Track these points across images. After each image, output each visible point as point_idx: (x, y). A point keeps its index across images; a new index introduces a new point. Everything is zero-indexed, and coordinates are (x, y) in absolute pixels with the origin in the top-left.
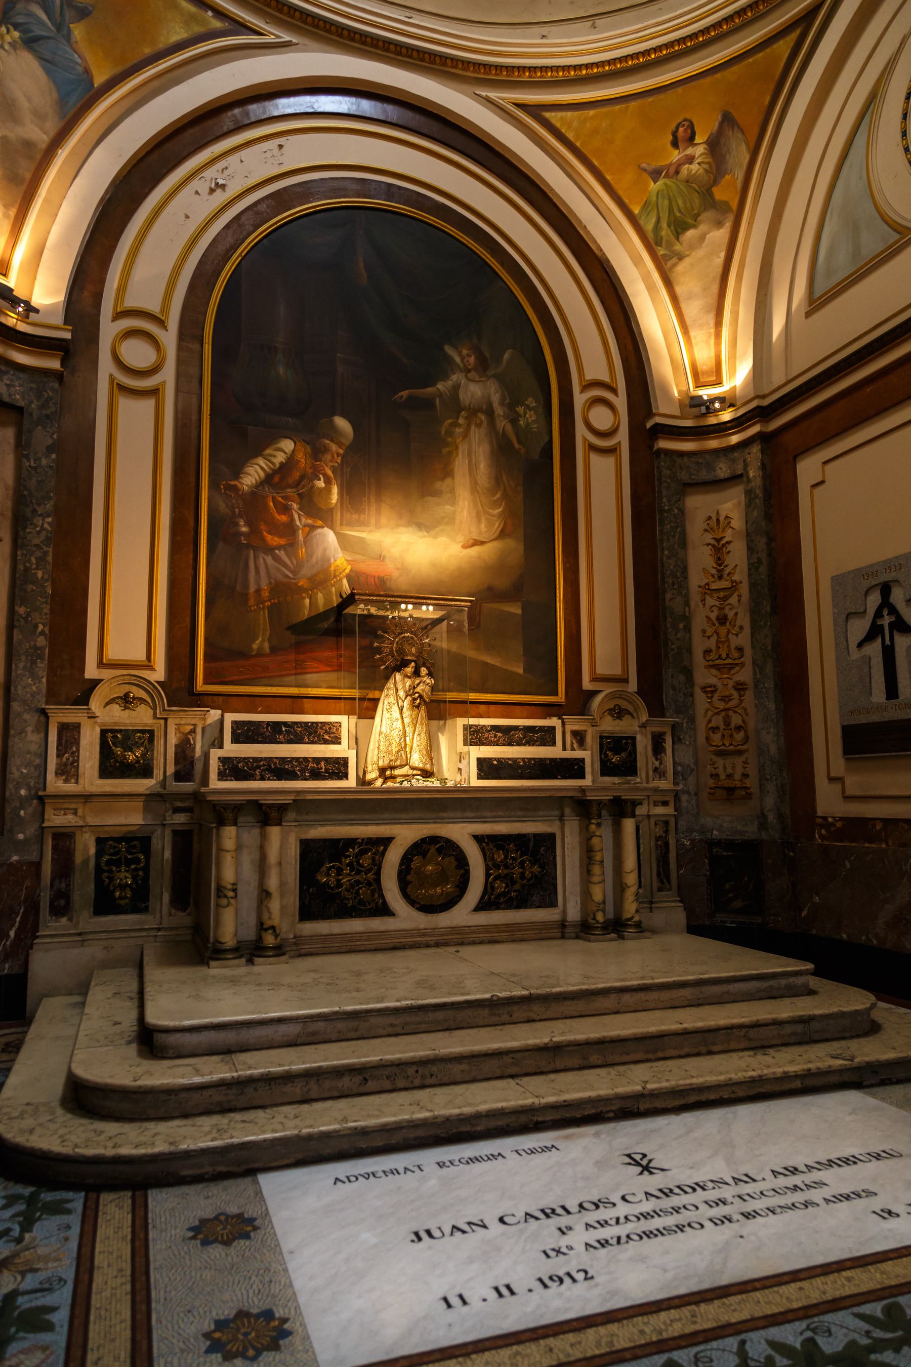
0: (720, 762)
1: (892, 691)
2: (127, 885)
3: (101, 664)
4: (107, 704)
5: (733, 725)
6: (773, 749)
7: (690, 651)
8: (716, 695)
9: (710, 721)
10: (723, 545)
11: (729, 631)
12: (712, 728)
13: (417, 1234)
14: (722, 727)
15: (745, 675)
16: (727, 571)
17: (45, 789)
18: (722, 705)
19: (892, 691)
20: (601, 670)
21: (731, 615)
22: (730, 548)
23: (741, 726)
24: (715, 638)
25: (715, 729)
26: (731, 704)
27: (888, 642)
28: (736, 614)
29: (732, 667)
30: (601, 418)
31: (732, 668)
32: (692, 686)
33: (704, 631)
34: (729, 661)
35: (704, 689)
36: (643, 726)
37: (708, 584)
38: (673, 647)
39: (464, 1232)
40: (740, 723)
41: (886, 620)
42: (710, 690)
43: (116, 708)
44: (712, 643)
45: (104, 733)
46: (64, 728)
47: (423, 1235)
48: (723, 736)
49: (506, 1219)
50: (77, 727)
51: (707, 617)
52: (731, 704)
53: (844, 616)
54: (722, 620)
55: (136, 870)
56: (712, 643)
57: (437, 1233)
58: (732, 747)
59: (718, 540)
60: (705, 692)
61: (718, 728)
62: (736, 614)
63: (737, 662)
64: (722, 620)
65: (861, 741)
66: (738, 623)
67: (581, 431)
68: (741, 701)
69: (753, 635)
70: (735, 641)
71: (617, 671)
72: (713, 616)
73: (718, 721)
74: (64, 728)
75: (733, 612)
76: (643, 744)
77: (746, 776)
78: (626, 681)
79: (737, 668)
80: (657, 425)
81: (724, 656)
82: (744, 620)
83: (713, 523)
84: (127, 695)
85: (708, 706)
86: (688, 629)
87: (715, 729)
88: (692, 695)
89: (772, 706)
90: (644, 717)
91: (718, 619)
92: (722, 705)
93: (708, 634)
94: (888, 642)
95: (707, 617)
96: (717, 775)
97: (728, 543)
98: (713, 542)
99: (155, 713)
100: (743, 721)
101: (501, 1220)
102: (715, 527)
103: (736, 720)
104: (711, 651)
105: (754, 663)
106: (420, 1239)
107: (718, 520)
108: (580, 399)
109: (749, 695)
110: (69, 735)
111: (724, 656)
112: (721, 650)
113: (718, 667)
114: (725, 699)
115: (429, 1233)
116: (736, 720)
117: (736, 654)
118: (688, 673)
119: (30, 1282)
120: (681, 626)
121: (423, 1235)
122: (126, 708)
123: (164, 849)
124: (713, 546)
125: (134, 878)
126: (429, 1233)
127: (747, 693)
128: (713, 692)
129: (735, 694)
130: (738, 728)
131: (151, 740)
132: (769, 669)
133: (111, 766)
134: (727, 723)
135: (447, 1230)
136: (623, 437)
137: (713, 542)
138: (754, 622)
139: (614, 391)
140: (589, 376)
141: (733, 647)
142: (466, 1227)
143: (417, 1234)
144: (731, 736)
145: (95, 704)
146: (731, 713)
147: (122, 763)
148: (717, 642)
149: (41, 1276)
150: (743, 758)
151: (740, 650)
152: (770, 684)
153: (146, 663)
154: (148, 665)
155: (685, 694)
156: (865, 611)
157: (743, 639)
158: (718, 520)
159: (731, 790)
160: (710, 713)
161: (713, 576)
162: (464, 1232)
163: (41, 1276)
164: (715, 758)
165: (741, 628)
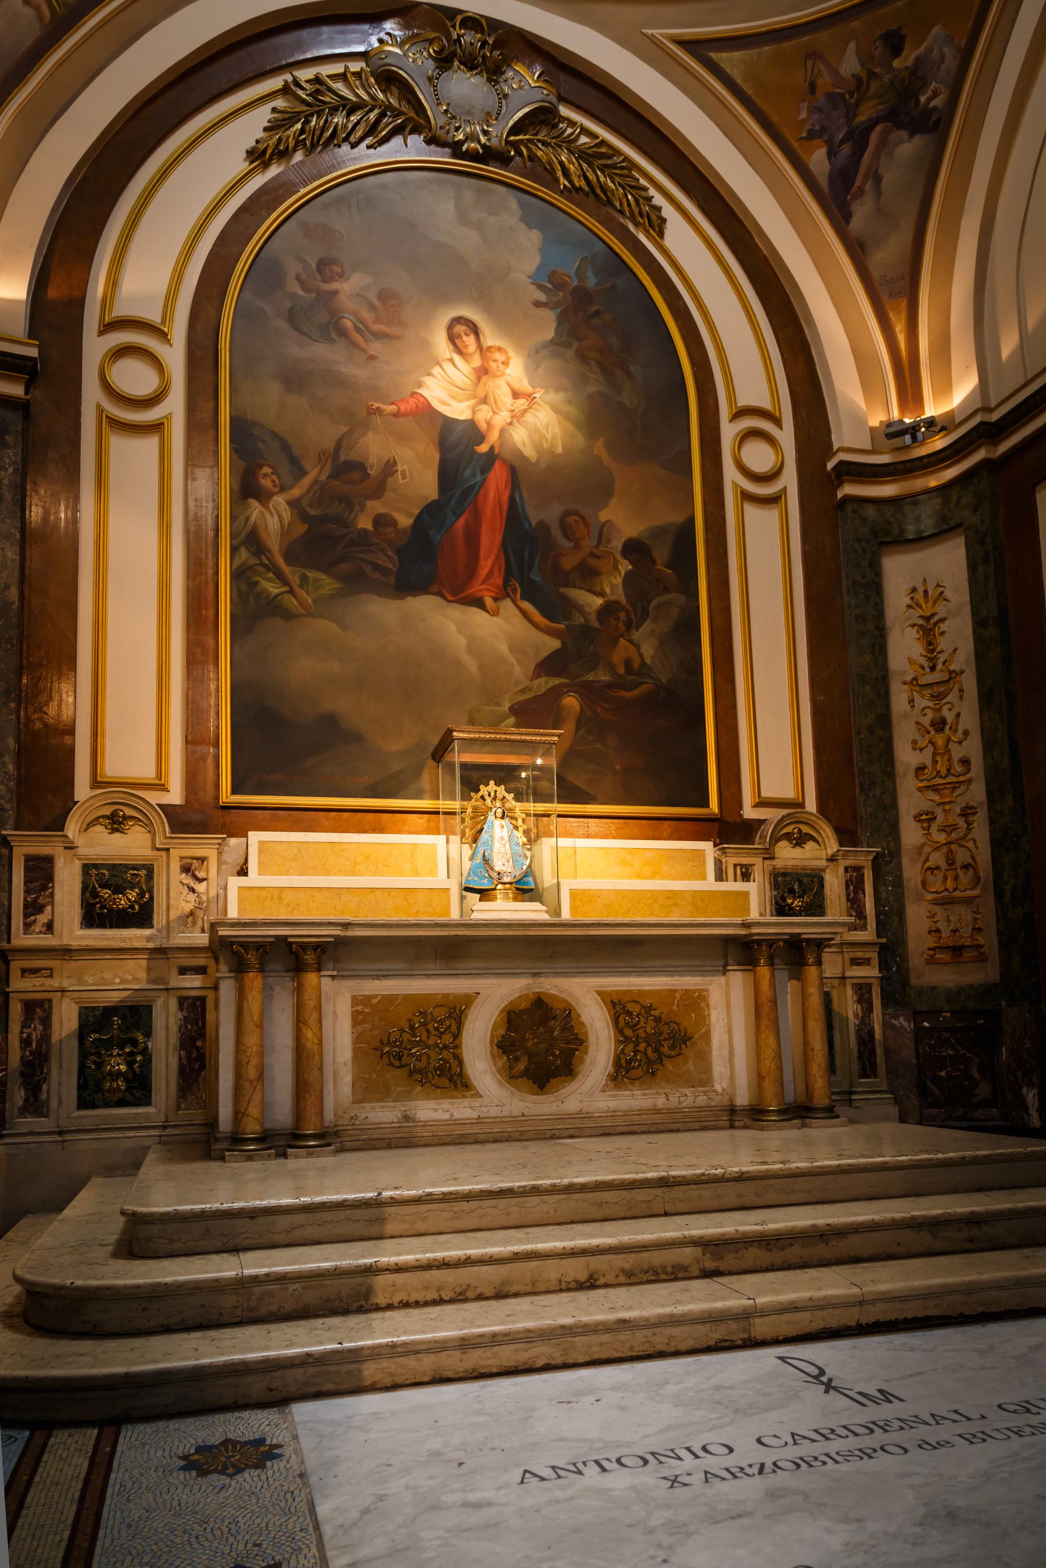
4: (90, 825)
5: (958, 864)
9: (927, 859)
10: (935, 624)
11: (949, 740)
12: (929, 868)
14: (944, 866)
16: (942, 658)
18: (942, 838)
21: (950, 717)
22: (943, 627)
23: (969, 865)
24: (930, 749)
28: (958, 715)
30: (759, 457)
31: (954, 788)
37: (915, 679)
43: (99, 831)
44: (926, 757)
48: (945, 878)
54: (939, 725)
56: (925, 757)
58: (957, 893)
59: (928, 619)
60: (920, 821)
61: (938, 868)
62: (958, 715)
63: (962, 778)
64: (939, 725)
66: (961, 728)
67: (730, 474)
70: (957, 752)
72: (926, 721)
73: (937, 859)
79: (963, 788)
80: (842, 463)
81: (943, 773)
83: (919, 597)
84: (114, 814)
85: (924, 840)
91: (933, 724)
92: (942, 838)
93: (920, 745)
95: (917, 723)
96: (938, 931)
97: (942, 620)
98: (921, 622)
99: (153, 840)
102: (922, 601)
104: (925, 767)
107: (926, 592)
108: (729, 431)
112: (939, 767)
113: (935, 789)
116: (962, 856)
117: (959, 768)
122: (114, 830)
124: (921, 626)
129: (962, 823)
130: (966, 867)
131: (150, 876)
133: (95, 915)
134: (951, 861)
136: (790, 480)
137: (921, 622)
139: (777, 422)
140: (744, 400)
144: (956, 878)
147: (111, 910)
148: (934, 754)
151: (965, 762)
158: (926, 592)
159: (957, 951)
160: (927, 849)
161: (923, 668)
164: (938, 909)
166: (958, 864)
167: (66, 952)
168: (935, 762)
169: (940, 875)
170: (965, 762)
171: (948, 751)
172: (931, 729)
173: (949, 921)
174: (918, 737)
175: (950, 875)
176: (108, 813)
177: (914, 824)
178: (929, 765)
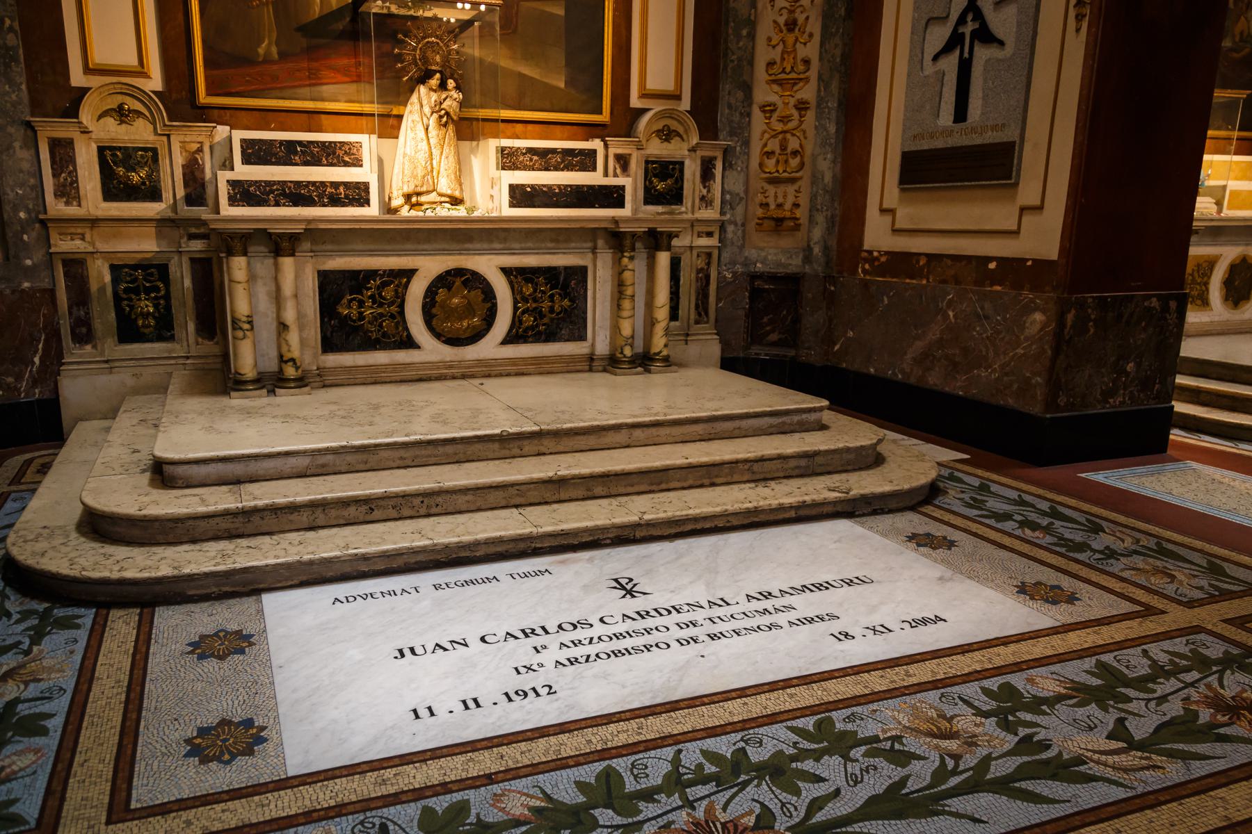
0: (771, 190)
1: (961, 114)
2: (148, 313)
3: (88, 70)
4: (100, 117)
5: (789, 150)
6: (828, 178)
7: (751, 63)
8: (775, 116)
9: (765, 145)
11: (797, 40)
12: (767, 152)
13: (401, 651)
14: (778, 151)
15: (808, 92)
17: (46, 213)
18: (779, 127)
19: (961, 114)
20: (652, 85)
21: (801, 19)
24: (780, 48)
25: (769, 154)
26: (791, 125)
27: (966, 55)
28: (807, 18)
29: (795, 82)
31: (795, 84)
32: (750, 105)
33: (769, 39)
34: (793, 75)
35: (762, 108)
36: (693, 150)
38: (734, 57)
39: (445, 650)
40: (797, 146)
41: (968, 29)
42: (768, 109)
43: (110, 122)
44: (776, 54)
45: (101, 150)
46: (55, 144)
47: (407, 652)
48: (778, 162)
49: (487, 638)
50: (70, 143)
51: (775, 22)
52: (791, 125)
53: (924, 22)
54: (791, 25)
55: (156, 298)
56: (776, 54)
57: (419, 650)
58: (786, 175)
60: (764, 112)
61: (773, 153)
62: (807, 18)
63: (802, 76)
65: (921, 170)
66: (808, 29)
68: (801, 122)
69: (822, 44)
70: (802, 52)
71: (669, 85)
72: (781, 20)
73: (774, 145)
74: (55, 144)
75: (804, 16)
76: (692, 170)
77: (796, 205)
78: (678, 97)
79: (801, 84)
81: (788, 70)
82: (815, 27)
84: (121, 107)
85: (765, 127)
86: (752, 36)
87: (769, 154)
88: (749, 115)
89: (832, 129)
90: (695, 140)
91: (786, 24)
92: (779, 127)
93: (773, 43)
94: (966, 55)
95: (775, 22)
96: (767, 204)
99: (155, 128)
100: (801, 146)
101: (483, 639)
103: (793, 144)
105: (820, 78)
106: (403, 656)
109: (810, 116)
110: (63, 153)
111: (788, 70)
112: (785, 64)
113: (779, 82)
114: (784, 119)
115: (412, 650)
116: (793, 144)
117: (801, 68)
118: (747, 89)
119: (33, 690)
120: (744, 32)
121: (407, 652)
122: (122, 122)
123: (183, 279)
125: (156, 306)
126: (412, 650)
127: (809, 112)
128: (772, 111)
129: (795, 113)
130: (795, 153)
131: (155, 159)
132: (834, 86)
133: (114, 189)
134: (783, 147)
135: (430, 648)
138: (825, 28)
141: (799, 58)
142: (448, 646)
143: (401, 651)
144: (786, 162)
145: (86, 116)
146: (788, 136)
147: (126, 184)
148: (783, 53)
149: (43, 685)
150: (796, 187)
151: (807, 62)
152: (833, 104)
153: (139, 69)
154: (142, 73)
155: (741, 114)
156: (948, 16)
157: (811, 50)
159: (779, 221)
160: (766, 136)
162: (445, 650)
163: (43, 685)
164: (767, 186)
165: (811, 35)
166: (789, 150)
167: (94, 222)
168: (783, 59)
169: (773, 161)
170: (807, 62)
171: (795, 50)
172: (784, 28)
173: (776, 197)
174: (773, 34)
175: (782, 158)
176: (115, 106)
177: (761, 115)
178: (778, 61)
